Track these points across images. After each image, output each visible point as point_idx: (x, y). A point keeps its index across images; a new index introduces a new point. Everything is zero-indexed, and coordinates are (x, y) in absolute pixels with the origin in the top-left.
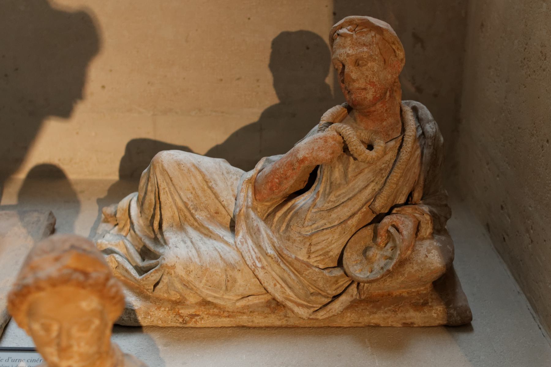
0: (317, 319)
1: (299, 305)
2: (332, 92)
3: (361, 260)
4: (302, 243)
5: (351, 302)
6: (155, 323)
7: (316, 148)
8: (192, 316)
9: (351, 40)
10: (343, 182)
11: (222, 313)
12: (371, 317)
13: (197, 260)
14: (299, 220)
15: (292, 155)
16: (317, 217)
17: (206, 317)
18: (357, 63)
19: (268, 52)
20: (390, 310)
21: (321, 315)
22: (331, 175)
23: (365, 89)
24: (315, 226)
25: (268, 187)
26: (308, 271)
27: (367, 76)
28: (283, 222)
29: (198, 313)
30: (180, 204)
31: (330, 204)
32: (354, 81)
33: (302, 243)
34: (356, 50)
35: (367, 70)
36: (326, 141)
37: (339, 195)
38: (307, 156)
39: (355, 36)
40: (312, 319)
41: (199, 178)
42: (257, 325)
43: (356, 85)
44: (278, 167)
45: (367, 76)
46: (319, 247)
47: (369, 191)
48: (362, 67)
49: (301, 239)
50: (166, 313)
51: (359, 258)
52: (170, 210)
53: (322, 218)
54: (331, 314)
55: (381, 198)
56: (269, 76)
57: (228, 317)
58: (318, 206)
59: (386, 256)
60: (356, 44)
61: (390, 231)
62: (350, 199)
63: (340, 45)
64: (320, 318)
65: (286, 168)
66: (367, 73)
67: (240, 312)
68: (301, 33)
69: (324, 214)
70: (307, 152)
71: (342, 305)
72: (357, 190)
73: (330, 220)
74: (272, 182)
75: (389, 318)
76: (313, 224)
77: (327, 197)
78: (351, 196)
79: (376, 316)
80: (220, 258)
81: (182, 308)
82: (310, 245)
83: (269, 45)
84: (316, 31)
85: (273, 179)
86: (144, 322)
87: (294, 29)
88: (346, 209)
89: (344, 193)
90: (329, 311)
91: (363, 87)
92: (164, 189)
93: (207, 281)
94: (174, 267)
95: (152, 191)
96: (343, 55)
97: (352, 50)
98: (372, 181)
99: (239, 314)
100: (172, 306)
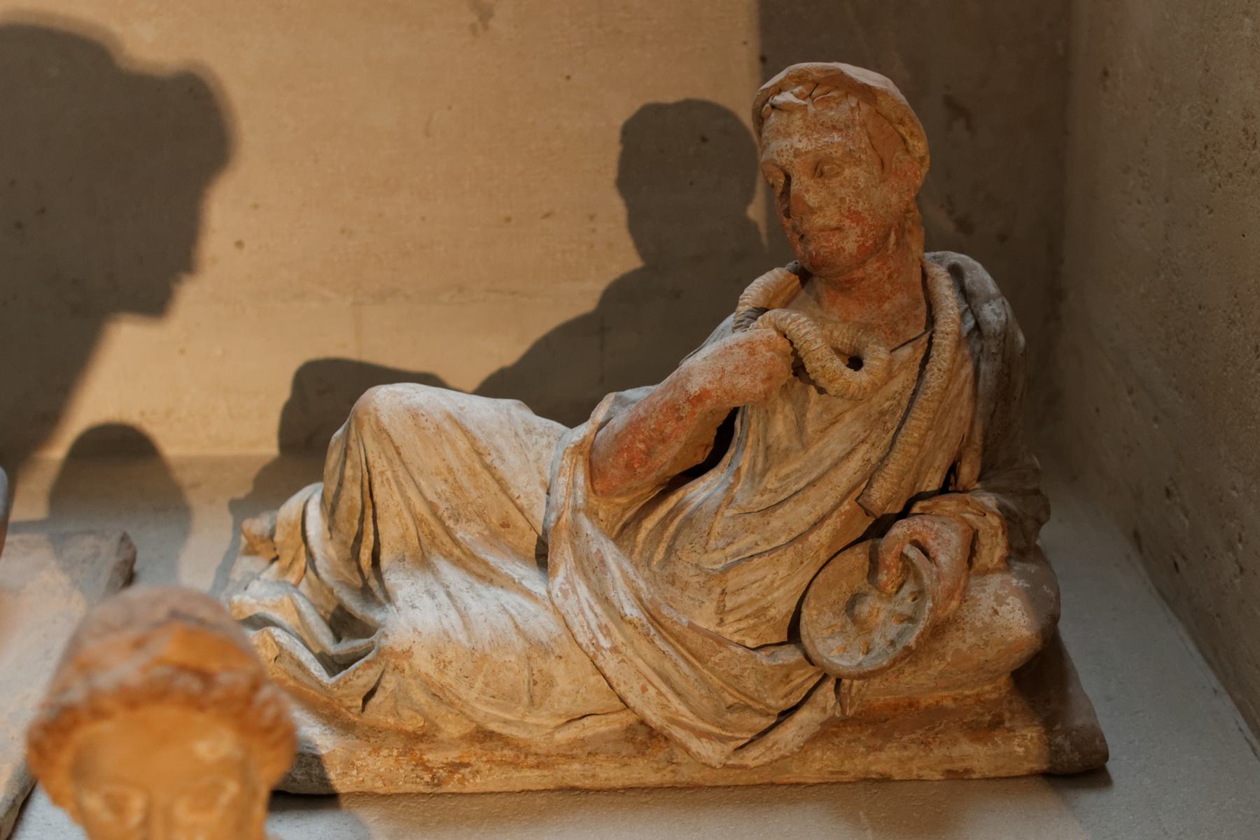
0: (744, 767)
1: (700, 734)
2: (764, 240)
3: (843, 626)
4: (705, 590)
5: (823, 724)
6: (367, 786)
7: (730, 368)
8: (454, 767)
9: (804, 119)
10: (796, 445)
11: (522, 757)
12: (870, 758)
13: (462, 637)
14: (694, 535)
15: (674, 385)
16: (737, 528)
17: (484, 768)
18: (818, 170)
19: (613, 152)
20: (913, 741)
21: (754, 757)
22: (766, 430)
23: (839, 229)
24: (734, 548)
25: (621, 461)
26: (720, 655)
27: (842, 200)
28: (659, 542)
29: (466, 760)
30: (421, 508)
31: (766, 497)
32: (812, 211)
35: (842, 185)
36: (752, 352)
37: (788, 476)
38: (709, 386)
39: (811, 109)
40: (734, 767)
41: (463, 445)
42: (606, 785)
43: (819, 221)
45: (842, 200)
46: (743, 598)
47: (855, 463)
49: (701, 579)
50: (392, 762)
52: (397, 520)
53: (749, 530)
54: (777, 755)
56: (617, 207)
57: (538, 766)
58: (739, 502)
59: (901, 615)
60: (815, 126)
61: (907, 557)
62: (812, 484)
63: (778, 130)
64: (752, 764)
65: (661, 417)
66: (842, 192)
67: (564, 756)
68: (688, 106)
69: (754, 520)
70: (710, 377)
71: (801, 732)
72: (828, 462)
73: (767, 535)
74: (629, 449)
75: (912, 759)
76: (729, 544)
77: (760, 482)
78: (814, 476)
79: (883, 756)
80: (514, 631)
81: (430, 749)
82: (723, 593)
83: (616, 135)
84: (722, 98)
85: (633, 442)
86: (343, 784)
87: (670, 99)
88: (803, 508)
89: (797, 470)
91: (833, 223)
92: (382, 473)
93: (487, 685)
94: (408, 654)
95: (354, 480)
96: (785, 154)
97: (805, 140)
99: (562, 760)
100: (405, 746)
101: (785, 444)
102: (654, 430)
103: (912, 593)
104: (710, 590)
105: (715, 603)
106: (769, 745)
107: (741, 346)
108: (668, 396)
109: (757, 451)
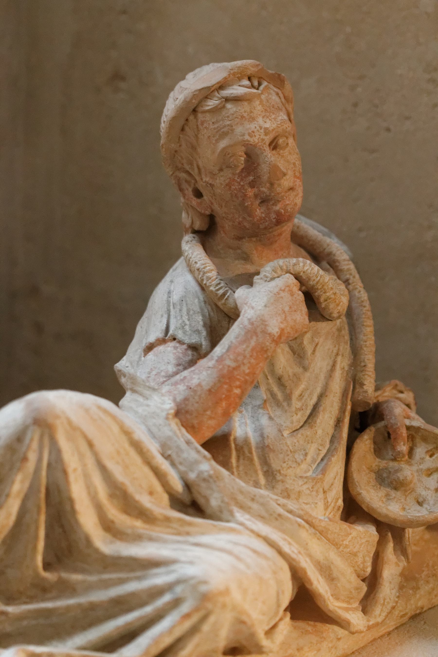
3: (387, 495)
4: (314, 493)
7: (287, 309)
9: (261, 103)
10: (299, 370)
12: (418, 596)
13: (241, 566)
14: (281, 456)
18: (274, 145)
22: (272, 365)
24: (309, 458)
26: (350, 537)
27: (294, 164)
28: (256, 471)
31: (300, 414)
33: (314, 493)
34: (275, 119)
35: (290, 153)
36: (292, 295)
38: (282, 326)
41: (116, 429)
44: (233, 365)
47: (338, 375)
48: (284, 148)
49: (309, 485)
51: (382, 492)
54: (389, 607)
55: (369, 376)
58: (285, 425)
59: (428, 469)
60: (269, 110)
61: (412, 427)
62: (321, 396)
63: (242, 117)
65: (253, 361)
69: (307, 431)
70: (280, 320)
72: (322, 377)
74: (228, 397)
76: (306, 455)
77: (289, 405)
78: (318, 390)
79: (422, 592)
82: (324, 492)
85: (229, 391)
88: (327, 415)
89: (306, 389)
90: (384, 604)
91: (291, 185)
92: (75, 470)
94: (226, 592)
96: (257, 134)
97: (268, 120)
98: (337, 354)
101: (290, 372)
102: (248, 374)
103: (427, 452)
104: (317, 492)
105: (323, 501)
106: (382, 602)
107: (284, 291)
108: (253, 343)
109: (268, 384)
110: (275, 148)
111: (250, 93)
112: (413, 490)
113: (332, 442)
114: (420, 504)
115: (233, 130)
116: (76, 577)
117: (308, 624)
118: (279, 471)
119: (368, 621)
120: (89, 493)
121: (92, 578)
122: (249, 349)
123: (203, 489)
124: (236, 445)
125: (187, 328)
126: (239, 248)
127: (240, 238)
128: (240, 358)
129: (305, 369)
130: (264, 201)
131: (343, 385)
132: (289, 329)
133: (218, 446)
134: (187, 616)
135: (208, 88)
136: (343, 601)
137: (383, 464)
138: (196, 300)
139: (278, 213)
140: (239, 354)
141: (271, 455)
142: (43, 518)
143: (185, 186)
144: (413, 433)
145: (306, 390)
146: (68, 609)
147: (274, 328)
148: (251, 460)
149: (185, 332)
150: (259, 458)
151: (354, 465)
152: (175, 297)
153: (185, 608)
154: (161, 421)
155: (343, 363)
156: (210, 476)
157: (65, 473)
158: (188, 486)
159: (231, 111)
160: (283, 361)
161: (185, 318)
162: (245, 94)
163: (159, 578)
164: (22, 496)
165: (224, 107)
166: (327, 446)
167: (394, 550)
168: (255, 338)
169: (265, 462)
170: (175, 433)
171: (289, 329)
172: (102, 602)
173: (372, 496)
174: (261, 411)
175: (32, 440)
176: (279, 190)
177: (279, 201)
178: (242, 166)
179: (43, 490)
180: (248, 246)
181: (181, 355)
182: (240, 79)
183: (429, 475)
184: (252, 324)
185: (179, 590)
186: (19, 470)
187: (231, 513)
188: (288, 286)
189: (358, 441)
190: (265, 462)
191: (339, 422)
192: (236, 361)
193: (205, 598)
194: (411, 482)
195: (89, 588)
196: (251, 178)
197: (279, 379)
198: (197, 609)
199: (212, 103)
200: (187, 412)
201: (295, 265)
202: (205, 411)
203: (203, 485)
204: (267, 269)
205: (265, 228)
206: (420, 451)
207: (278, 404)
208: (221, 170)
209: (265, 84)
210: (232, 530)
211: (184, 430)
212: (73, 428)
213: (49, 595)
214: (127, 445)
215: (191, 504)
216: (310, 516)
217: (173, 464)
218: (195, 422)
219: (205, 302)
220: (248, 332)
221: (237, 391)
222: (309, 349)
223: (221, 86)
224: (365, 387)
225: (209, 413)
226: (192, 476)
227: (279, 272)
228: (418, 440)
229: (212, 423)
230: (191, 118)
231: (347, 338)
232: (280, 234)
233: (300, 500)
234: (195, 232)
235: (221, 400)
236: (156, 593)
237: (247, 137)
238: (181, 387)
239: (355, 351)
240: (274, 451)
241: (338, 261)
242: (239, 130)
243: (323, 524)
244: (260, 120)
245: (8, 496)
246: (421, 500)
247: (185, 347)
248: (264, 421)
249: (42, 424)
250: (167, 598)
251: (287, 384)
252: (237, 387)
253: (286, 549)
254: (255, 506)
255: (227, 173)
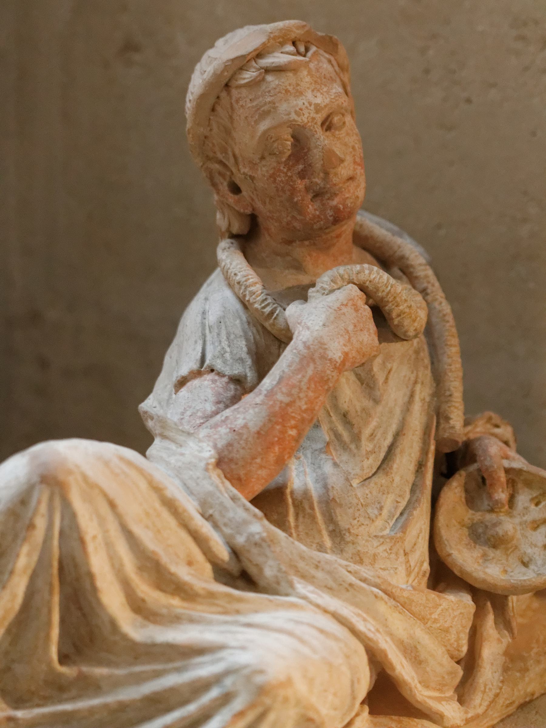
3: (484, 556)
4: (393, 556)
7: (351, 328)
9: (310, 73)
10: (368, 404)
12: (527, 679)
13: (306, 651)
14: (351, 511)
16: (375, 493)
18: (328, 125)
22: (335, 398)
24: (385, 512)
26: (440, 609)
27: (353, 148)
28: (320, 532)
32: (342, 161)
33: (393, 556)
35: (348, 134)
36: (357, 310)
38: (346, 349)
41: (143, 485)
44: (287, 400)
47: (417, 407)
48: (340, 128)
49: (387, 547)
51: (478, 552)
54: (491, 695)
55: (456, 408)
58: (353, 472)
59: (534, 522)
60: (320, 81)
62: (397, 435)
63: (287, 91)
65: (311, 394)
69: (381, 479)
70: (342, 342)
72: (398, 411)
74: (281, 441)
76: (381, 508)
77: (358, 447)
78: (394, 428)
79: (531, 674)
82: (406, 554)
85: (283, 432)
89: (378, 427)
90: (484, 692)
91: (350, 173)
92: (94, 537)
94: (288, 682)
96: (306, 112)
97: (318, 94)
98: (416, 382)
102: (306, 411)
103: (532, 500)
104: (397, 554)
105: (404, 567)
106: (483, 689)
107: (346, 305)
108: (310, 372)
109: (331, 422)
110: (329, 129)
111: (295, 62)
112: (516, 547)
113: (413, 491)
114: (525, 564)
115: (275, 108)
116: (100, 671)
117: (392, 720)
118: (349, 530)
119: (466, 712)
120: (113, 566)
121: (120, 672)
122: (305, 380)
123: (255, 556)
124: (293, 500)
125: (227, 356)
126: (288, 254)
127: (289, 242)
128: (295, 391)
129: (377, 402)
130: (318, 195)
131: (424, 419)
132: (354, 353)
133: (271, 501)
134: (240, 714)
135: (243, 57)
136: (434, 689)
137: (478, 516)
138: (238, 321)
139: (336, 210)
140: (294, 386)
141: (338, 511)
142: (56, 599)
143: (218, 179)
144: (514, 477)
145: (379, 428)
146: (91, 711)
147: (336, 351)
148: (313, 518)
149: (225, 362)
150: (323, 514)
151: (442, 519)
152: (212, 318)
153: (237, 705)
154: (199, 473)
155: (423, 393)
156: (263, 540)
157: (82, 541)
158: (235, 553)
159: (273, 85)
160: (349, 392)
161: (225, 343)
162: (290, 63)
163: (204, 669)
164: (29, 572)
165: (263, 79)
166: (407, 496)
167: (495, 623)
168: (312, 366)
169: (330, 519)
170: (217, 487)
171: (354, 353)
172: (134, 702)
173: (465, 557)
174: (323, 456)
175: (39, 502)
176: (335, 180)
177: (336, 195)
178: (289, 153)
179: (55, 564)
180: (299, 251)
181: (221, 390)
182: (282, 44)
183: (535, 529)
184: (308, 348)
185: (228, 682)
186: (25, 540)
187: (291, 585)
188: (351, 300)
189: (445, 489)
190: (330, 519)
191: (420, 466)
192: (289, 394)
193: (262, 691)
194: (513, 538)
195: (117, 684)
196: (301, 167)
197: (345, 415)
198: (252, 706)
199: (248, 76)
200: (231, 460)
201: (358, 273)
202: (254, 458)
203: (255, 551)
204: (325, 280)
205: (321, 229)
206: (523, 499)
207: (345, 447)
208: (263, 158)
209: (313, 49)
210: (293, 606)
211: (228, 483)
212: (90, 485)
213: (65, 696)
214: (157, 505)
215: (240, 575)
216: (390, 584)
217: (216, 526)
218: (242, 473)
219: (249, 323)
220: (303, 358)
221: (293, 433)
222: (380, 378)
223: (259, 55)
224: (452, 422)
225: (258, 460)
226: (240, 540)
227: (340, 283)
228: (520, 485)
229: (263, 473)
230: (224, 94)
231: (427, 361)
232: (339, 236)
233: (377, 566)
234: (233, 236)
235: (273, 444)
236: (200, 687)
237: (293, 116)
238: (223, 430)
239: (438, 378)
240: (341, 505)
241: (412, 266)
242: (283, 107)
243: (405, 594)
244: (309, 95)
245: (12, 573)
246: (526, 559)
247: (225, 379)
248: (328, 468)
249: (51, 481)
250: (214, 693)
251: (354, 421)
252: (292, 428)
253: (361, 626)
254: (319, 574)
255: (271, 162)
